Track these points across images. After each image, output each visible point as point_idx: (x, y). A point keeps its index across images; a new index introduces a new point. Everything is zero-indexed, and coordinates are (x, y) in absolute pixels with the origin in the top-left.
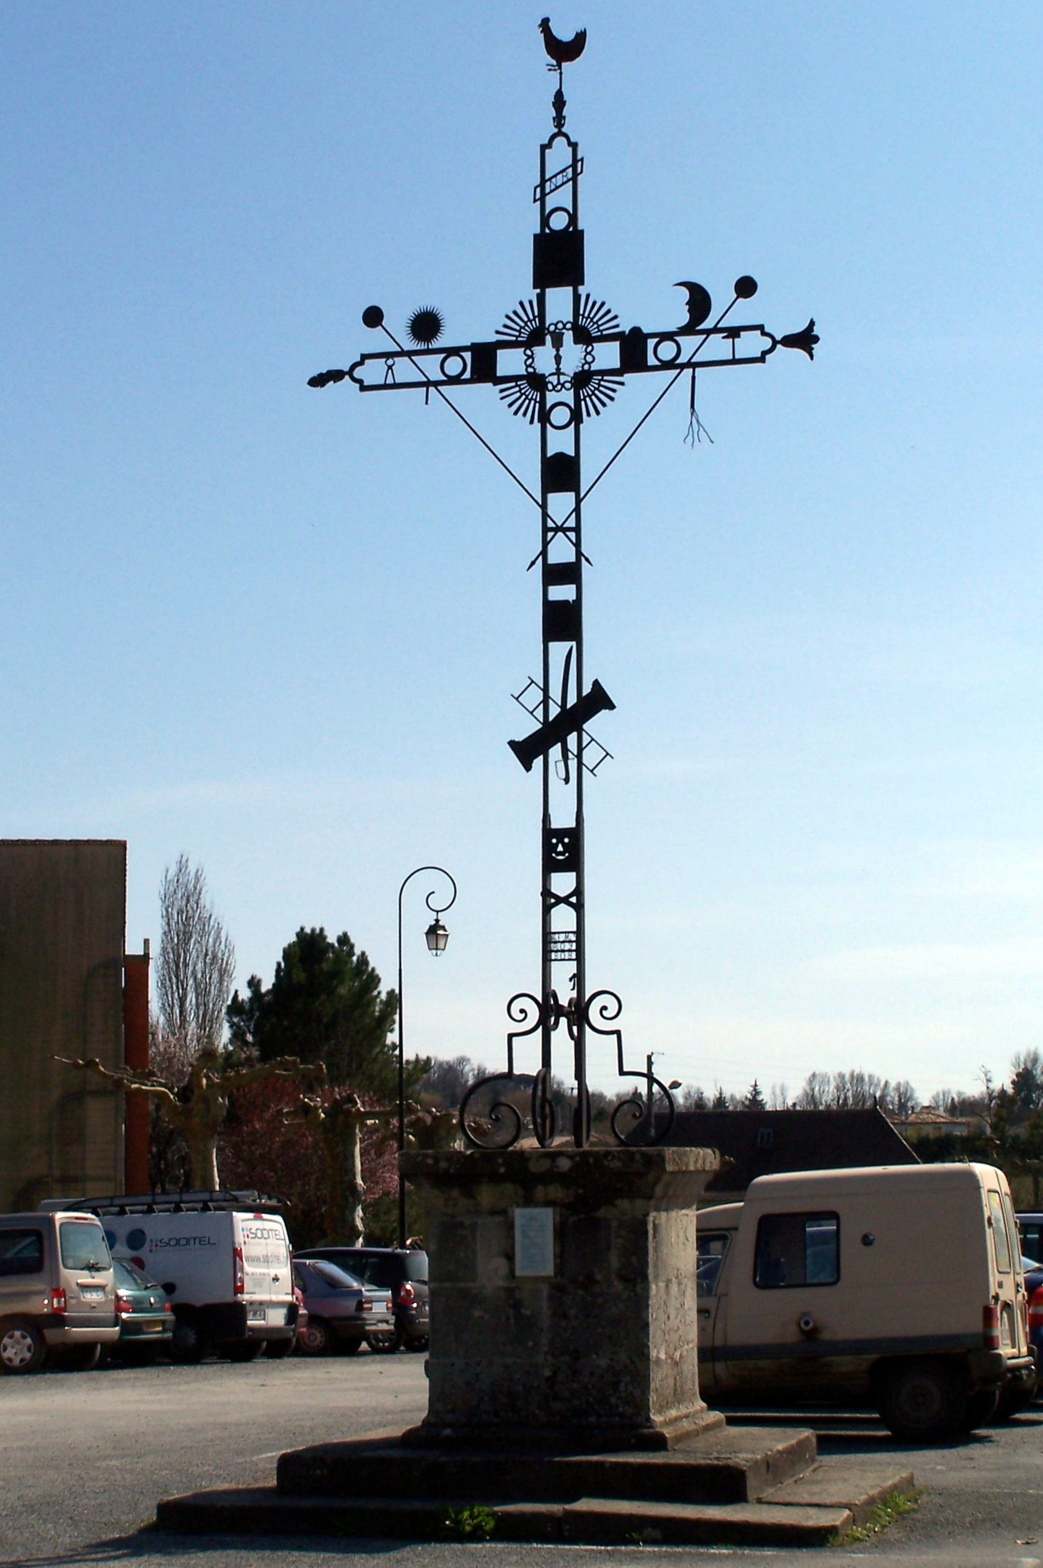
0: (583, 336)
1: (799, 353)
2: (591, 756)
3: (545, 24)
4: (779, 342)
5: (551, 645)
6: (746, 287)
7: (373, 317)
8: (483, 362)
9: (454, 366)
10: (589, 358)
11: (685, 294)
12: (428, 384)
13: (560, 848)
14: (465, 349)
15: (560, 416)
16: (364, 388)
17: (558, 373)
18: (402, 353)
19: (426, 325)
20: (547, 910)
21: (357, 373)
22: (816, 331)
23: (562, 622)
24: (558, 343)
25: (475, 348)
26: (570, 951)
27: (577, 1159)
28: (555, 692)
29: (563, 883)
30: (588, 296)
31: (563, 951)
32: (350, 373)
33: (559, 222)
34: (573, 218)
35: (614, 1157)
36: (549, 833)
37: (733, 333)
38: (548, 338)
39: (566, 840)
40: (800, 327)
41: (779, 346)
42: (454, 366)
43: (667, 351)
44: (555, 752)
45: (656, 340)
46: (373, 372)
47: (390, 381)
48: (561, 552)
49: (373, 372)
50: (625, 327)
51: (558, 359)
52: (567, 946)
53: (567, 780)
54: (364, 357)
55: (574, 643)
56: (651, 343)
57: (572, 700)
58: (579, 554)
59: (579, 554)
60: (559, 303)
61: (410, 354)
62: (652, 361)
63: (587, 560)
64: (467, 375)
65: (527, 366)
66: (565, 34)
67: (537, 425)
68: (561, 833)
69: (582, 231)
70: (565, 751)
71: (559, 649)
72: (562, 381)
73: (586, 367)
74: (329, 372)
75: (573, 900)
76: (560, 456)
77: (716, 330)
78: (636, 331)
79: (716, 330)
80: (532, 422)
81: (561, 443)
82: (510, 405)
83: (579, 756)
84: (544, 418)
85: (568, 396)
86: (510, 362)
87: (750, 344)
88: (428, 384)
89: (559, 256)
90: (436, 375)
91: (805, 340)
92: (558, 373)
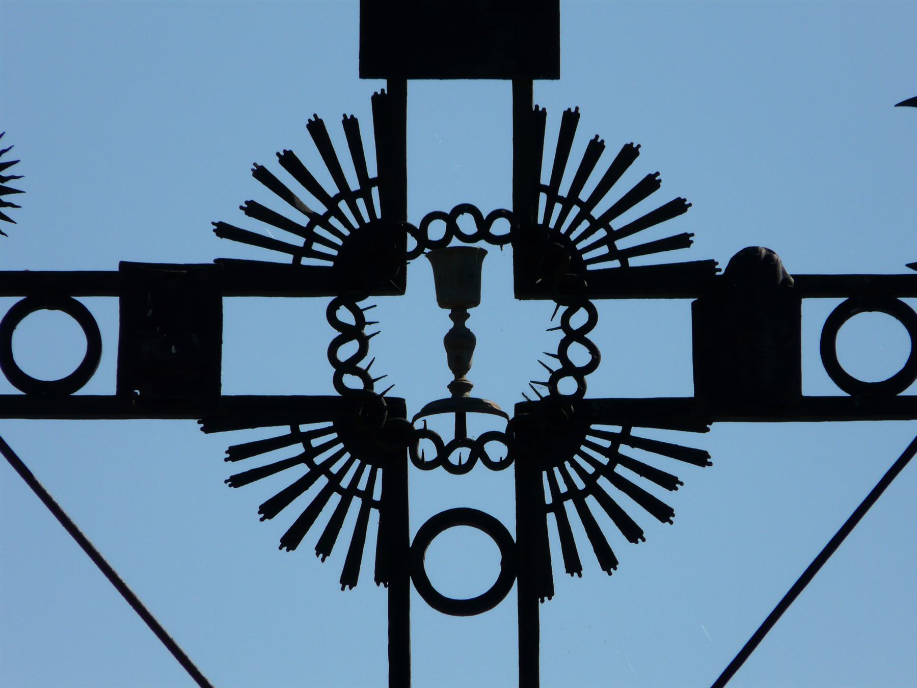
10: (578, 355)
14: (96, 283)
17: (460, 402)
24: (459, 287)
38: (420, 273)
45: (834, 302)
51: (460, 347)
56: (815, 312)
60: (460, 145)
62: (815, 382)
72: (473, 433)
78: (755, 264)
92: (460, 402)
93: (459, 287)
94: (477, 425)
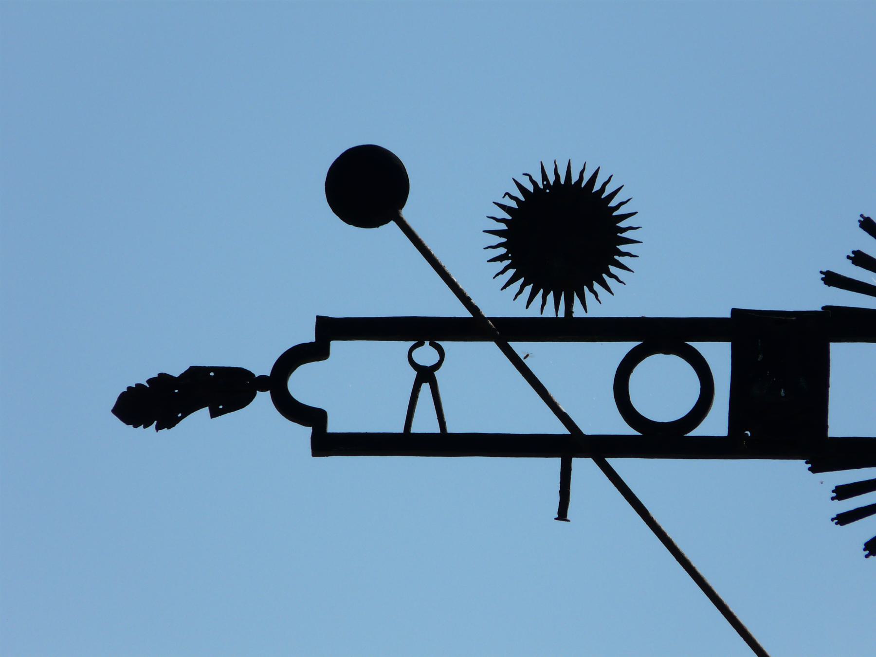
7: (367, 187)
9: (665, 388)
12: (569, 445)
16: (327, 444)
18: (474, 327)
19: (563, 233)
21: (304, 384)
25: (746, 329)
32: (276, 383)
42: (665, 388)
46: (362, 386)
47: (425, 423)
49: (362, 386)
54: (332, 329)
61: (505, 332)
64: (716, 424)
74: (195, 374)
88: (569, 445)
90: (602, 420)
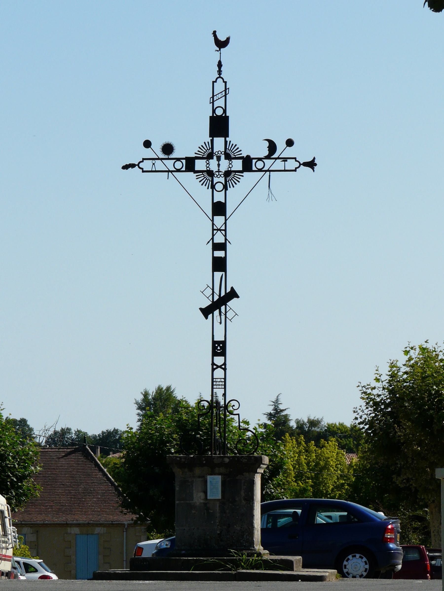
0: (228, 157)
1: (309, 169)
2: (229, 315)
3: (214, 33)
4: (302, 164)
5: (215, 273)
6: (290, 143)
7: (147, 144)
8: (190, 165)
9: (179, 165)
10: (231, 166)
11: (267, 144)
12: (169, 171)
13: (219, 348)
15: (219, 187)
17: (219, 171)
19: (168, 149)
20: (213, 370)
21: (141, 165)
22: (316, 162)
23: (219, 265)
24: (219, 159)
25: (187, 159)
26: (222, 385)
27: (231, 459)
28: (217, 290)
29: (219, 360)
30: (230, 142)
31: (219, 385)
32: (138, 165)
33: (219, 112)
34: (225, 111)
35: (244, 458)
36: (214, 343)
37: (285, 160)
38: (215, 157)
39: (221, 345)
40: (309, 159)
41: (301, 166)
42: (179, 165)
43: (260, 165)
44: (217, 312)
46: (147, 165)
47: (154, 169)
48: (219, 238)
49: (147, 165)
50: (244, 155)
51: (219, 165)
52: (221, 383)
53: (221, 323)
55: (224, 273)
56: (254, 161)
57: (223, 294)
58: (226, 239)
59: (226, 239)
60: (219, 143)
61: (161, 159)
63: (229, 242)
64: (184, 169)
65: (207, 167)
66: (222, 38)
67: (210, 190)
68: (219, 343)
69: (228, 116)
70: (220, 312)
71: (218, 275)
73: (229, 169)
74: (130, 164)
75: (223, 367)
76: (219, 203)
77: (278, 158)
78: (248, 157)
79: (278, 158)
80: (208, 188)
81: (219, 197)
82: (200, 181)
83: (225, 315)
84: (213, 187)
85: (222, 180)
86: (200, 165)
87: (291, 164)
88: (169, 171)
89: (219, 125)
91: (311, 164)
92: (219, 171)
93: (219, 159)
94: (220, 173)
